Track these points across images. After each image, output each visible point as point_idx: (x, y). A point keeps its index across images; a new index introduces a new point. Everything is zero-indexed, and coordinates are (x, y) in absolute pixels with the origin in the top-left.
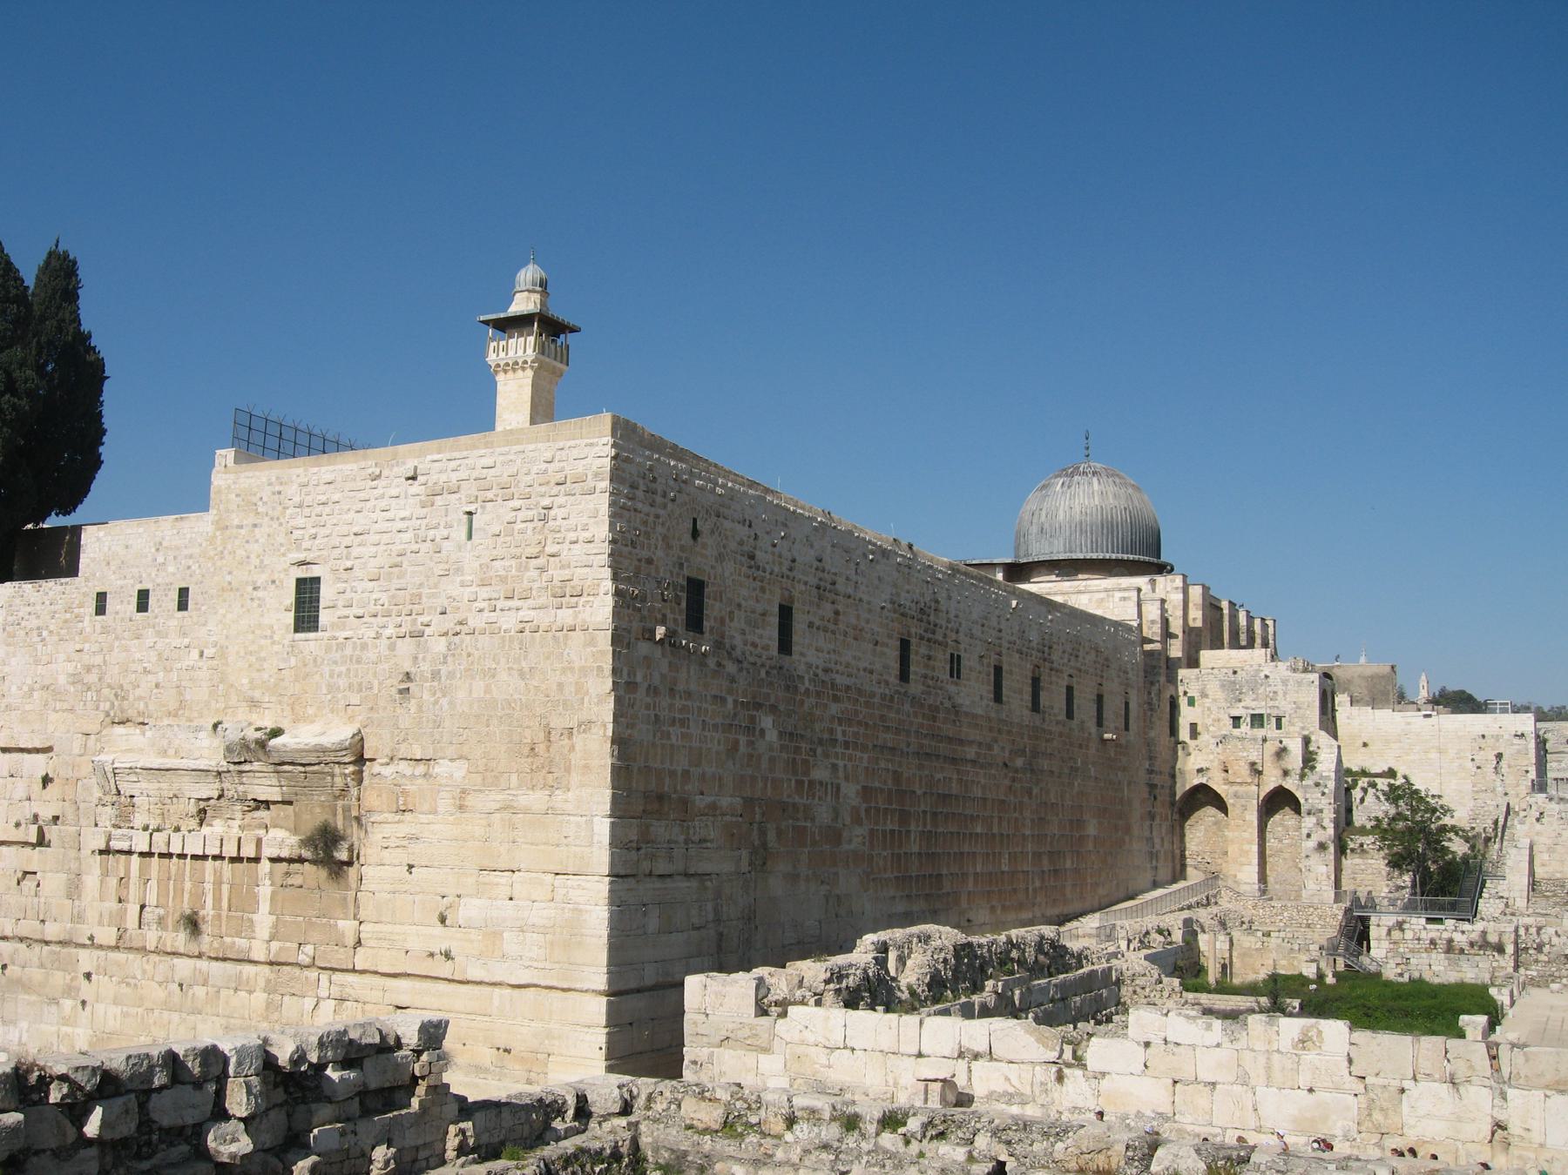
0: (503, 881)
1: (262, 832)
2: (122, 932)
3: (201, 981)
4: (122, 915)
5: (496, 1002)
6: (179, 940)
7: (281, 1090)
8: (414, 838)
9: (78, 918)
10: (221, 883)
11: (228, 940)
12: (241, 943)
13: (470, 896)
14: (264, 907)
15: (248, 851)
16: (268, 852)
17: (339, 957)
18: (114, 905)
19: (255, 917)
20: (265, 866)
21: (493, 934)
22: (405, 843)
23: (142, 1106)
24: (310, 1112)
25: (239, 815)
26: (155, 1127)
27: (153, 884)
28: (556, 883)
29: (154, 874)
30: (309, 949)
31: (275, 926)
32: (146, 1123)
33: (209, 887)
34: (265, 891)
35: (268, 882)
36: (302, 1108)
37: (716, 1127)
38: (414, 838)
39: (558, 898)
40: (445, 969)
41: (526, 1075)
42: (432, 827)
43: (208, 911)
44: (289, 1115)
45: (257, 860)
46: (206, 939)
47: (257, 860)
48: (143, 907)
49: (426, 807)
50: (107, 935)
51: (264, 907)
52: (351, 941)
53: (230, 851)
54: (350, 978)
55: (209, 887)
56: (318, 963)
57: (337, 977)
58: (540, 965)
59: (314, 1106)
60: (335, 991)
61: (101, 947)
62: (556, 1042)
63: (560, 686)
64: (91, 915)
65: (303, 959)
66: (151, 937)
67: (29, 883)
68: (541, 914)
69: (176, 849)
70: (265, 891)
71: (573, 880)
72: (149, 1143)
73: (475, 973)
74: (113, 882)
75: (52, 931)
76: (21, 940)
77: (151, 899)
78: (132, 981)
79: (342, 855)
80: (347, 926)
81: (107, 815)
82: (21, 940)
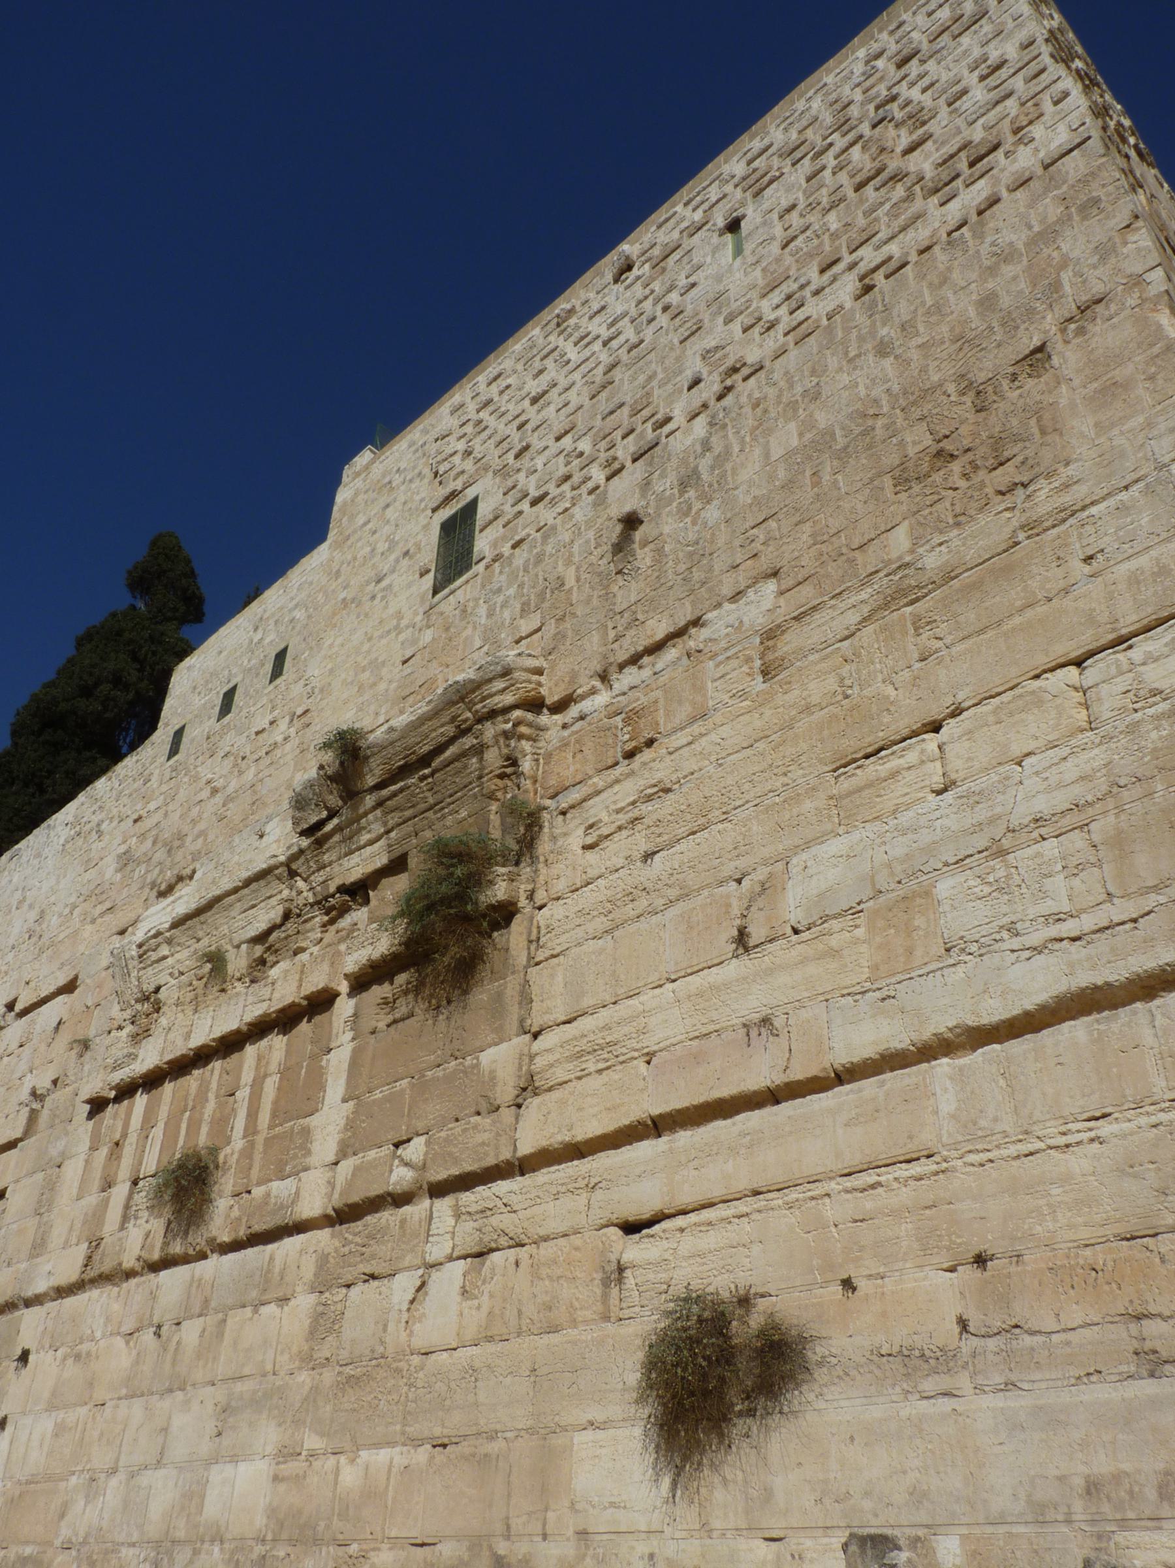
0: (912, 757)
5: (947, 1103)
14: (335, 1088)
20: (345, 1007)
21: (896, 902)
31: (350, 1125)
33: (243, 1094)
41: (1122, 1335)
49: (683, 713)
51: (335, 1088)
52: (506, 1092)
55: (243, 1094)
58: (1088, 922)
60: (468, 1235)
63: (987, 303)
65: (401, 1177)
79: (499, 891)
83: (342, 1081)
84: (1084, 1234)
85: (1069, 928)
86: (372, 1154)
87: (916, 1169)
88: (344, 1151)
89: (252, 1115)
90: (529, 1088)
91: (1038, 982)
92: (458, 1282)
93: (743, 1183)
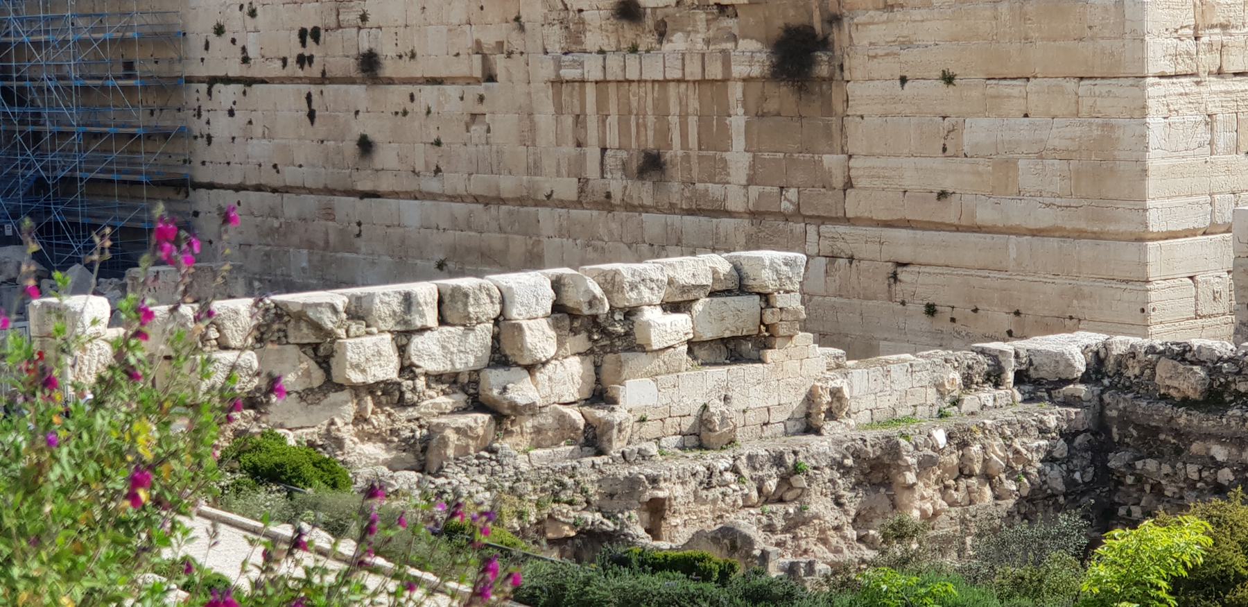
1: (729, 45)
2: (583, 182)
3: (675, 241)
4: (581, 161)
6: (643, 192)
7: (583, 336)
8: (907, 44)
9: (535, 168)
10: (687, 115)
11: (700, 186)
12: (715, 190)
13: (974, 114)
14: (739, 142)
15: (715, 71)
16: (738, 70)
17: (825, 202)
18: (569, 149)
19: (727, 155)
22: (896, 49)
23: (402, 350)
24: (620, 364)
25: (701, 26)
26: (418, 371)
27: (613, 120)
28: (1081, 91)
29: (613, 108)
30: (792, 194)
31: (753, 167)
32: (407, 369)
33: (674, 120)
34: (738, 121)
35: (740, 111)
36: (610, 357)
37: (1192, 395)
38: (907, 44)
39: (1084, 110)
40: (949, 213)
42: (927, 25)
43: (674, 152)
44: (597, 367)
45: (725, 81)
46: (675, 186)
47: (725, 81)
48: (604, 150)
50: (567, 188)
51: (739, 142)
52: (838, 182)
53: (693, 71)
54: (842, 229)
55: (674, 120)
56: (804, 211)
57: (826, 229)
58: (1064, 202)
59: (623, 356)
61: (563, 204)
62: (1086, 303)
64: (548, 164)
65: (786, 206)
66: (616, 185)
67: (477, 130)
68: (1060, 134)
69: (632, 74)
70: (738, 121)
71: (1102, 87)
72: (414, 390)
73: (985, 214)
74: (569, 121)
75: (507, 185)
76: (476, 199)
77: (612, 139)
78: (600, 243)
80: (831, 161)
81: (555, 38)
82: (476, 199)
83: (742, 138)
84: (1046, 313)
85: (1058, 201)
86: (768, 189)
87: (1002, 275)
88: (751, 181)
89: (684, 136)
90: (849, 184)
91: (1045, 218)
92: (823, 269)
93: (942, 262)
